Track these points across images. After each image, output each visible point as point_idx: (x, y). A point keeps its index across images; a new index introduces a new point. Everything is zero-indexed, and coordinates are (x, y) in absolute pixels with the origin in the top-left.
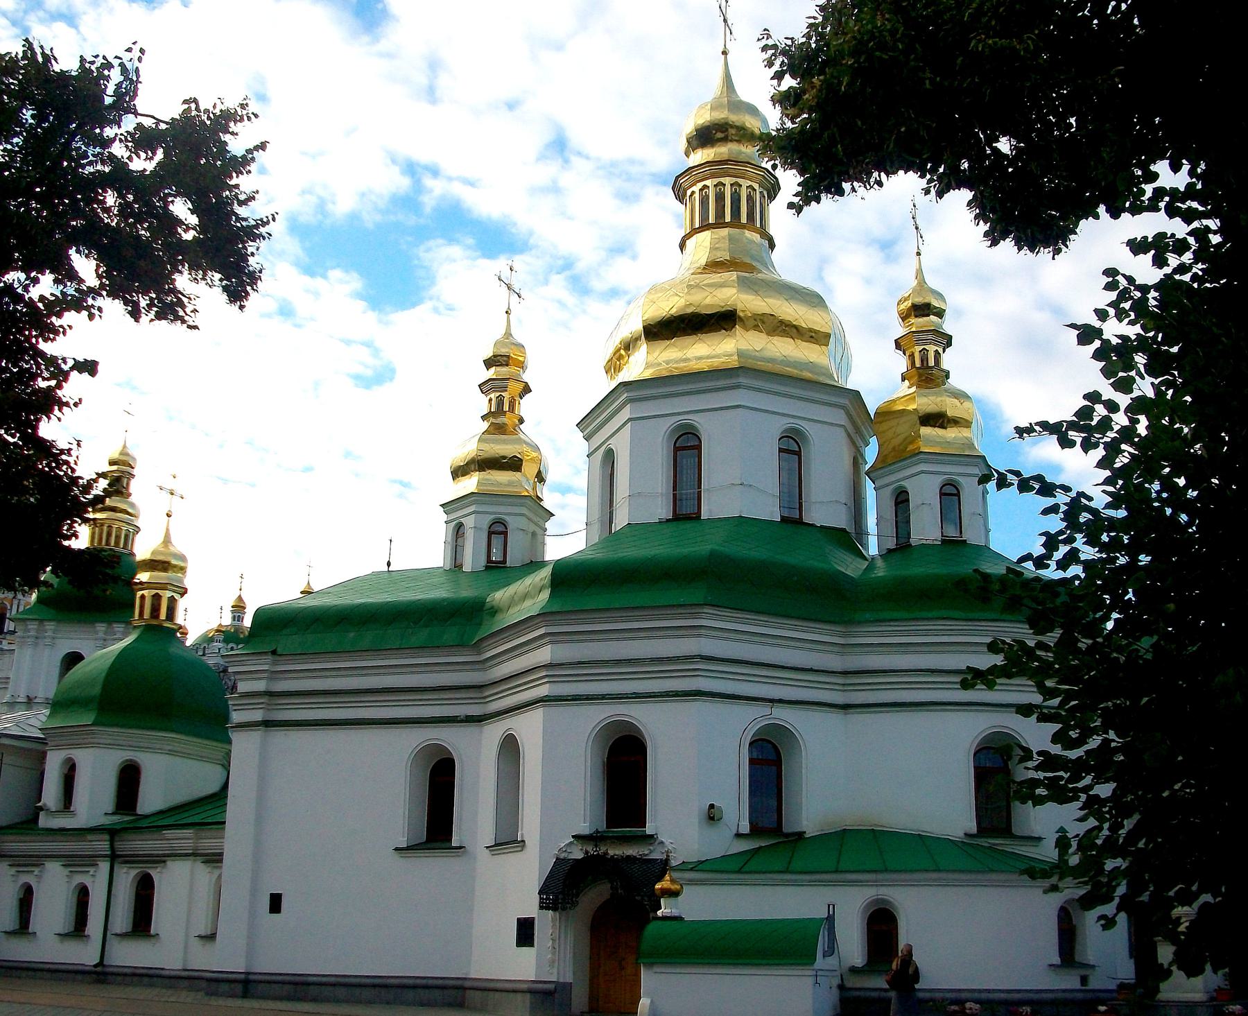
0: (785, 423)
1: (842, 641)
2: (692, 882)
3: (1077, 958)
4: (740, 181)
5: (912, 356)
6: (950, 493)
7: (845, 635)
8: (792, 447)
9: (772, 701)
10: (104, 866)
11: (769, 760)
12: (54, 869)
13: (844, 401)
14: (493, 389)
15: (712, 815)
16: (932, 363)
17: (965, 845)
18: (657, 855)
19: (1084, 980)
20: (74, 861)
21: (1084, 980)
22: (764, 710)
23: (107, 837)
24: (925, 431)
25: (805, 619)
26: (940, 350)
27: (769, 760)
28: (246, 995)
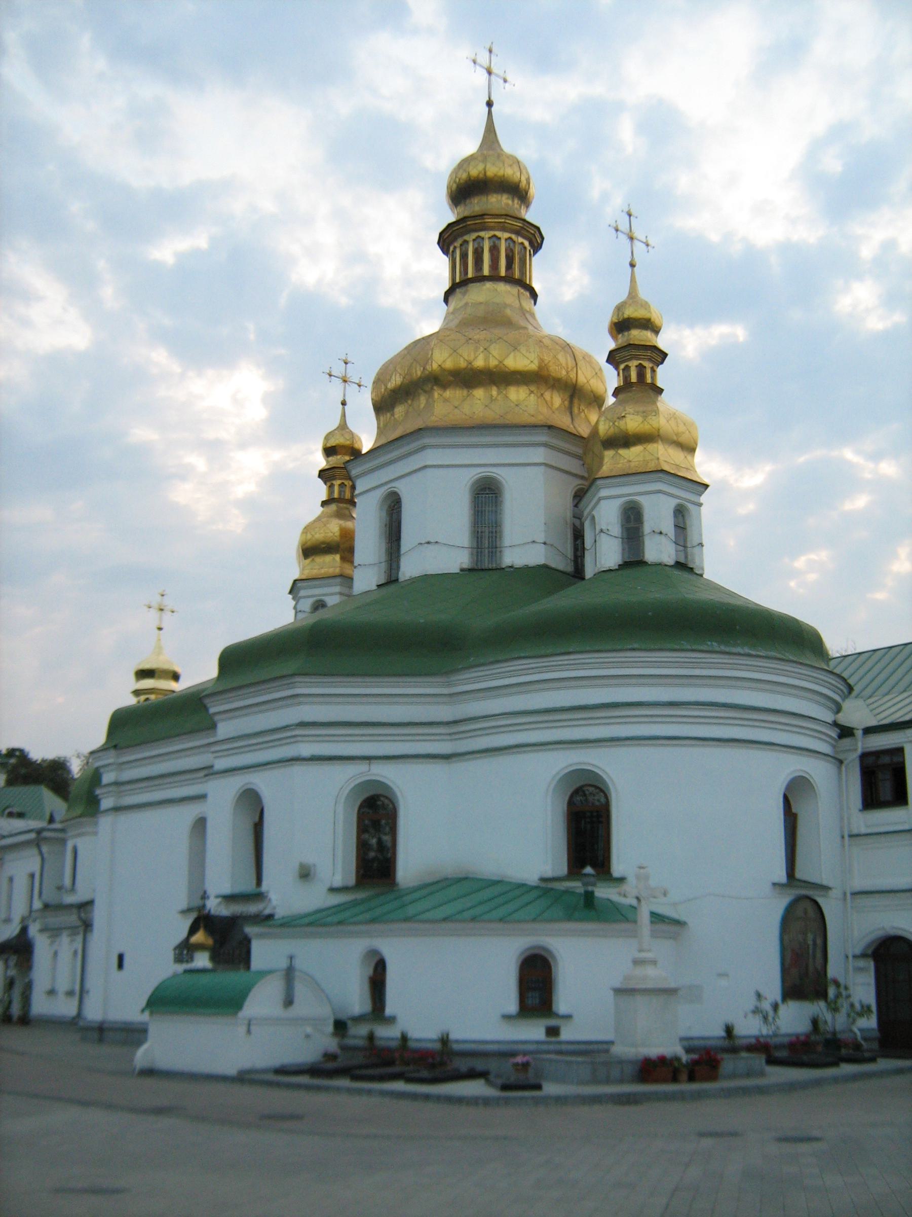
0: (472, 475)
1: (445, 691)
2: (261, 936)
3: (554, 1008)
4: (482, 234)
5: (618, 375)
6: (632, 517)
7: (449, 685)
8: (487, 495)
9: (368, 758)
10: (82, 933)
11: (376, 815)
12: (65, 939)
13: (543, 438)
14: (334, 478)
15: (305, 874)
16: (634, 378)
17: (545, 889)
18: (267, 912)
19: (553, 1031)
20: (73, 931)
21: (553, 1031)
22: (362, 767)
23: (75, 911)
24: (609, 454)
25: (400, 675)
26: (646, 364)
27: (376, 815)
28: (101, 1040)
